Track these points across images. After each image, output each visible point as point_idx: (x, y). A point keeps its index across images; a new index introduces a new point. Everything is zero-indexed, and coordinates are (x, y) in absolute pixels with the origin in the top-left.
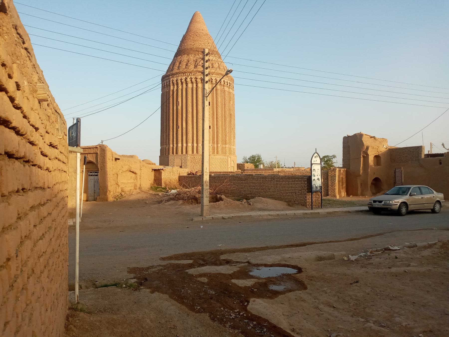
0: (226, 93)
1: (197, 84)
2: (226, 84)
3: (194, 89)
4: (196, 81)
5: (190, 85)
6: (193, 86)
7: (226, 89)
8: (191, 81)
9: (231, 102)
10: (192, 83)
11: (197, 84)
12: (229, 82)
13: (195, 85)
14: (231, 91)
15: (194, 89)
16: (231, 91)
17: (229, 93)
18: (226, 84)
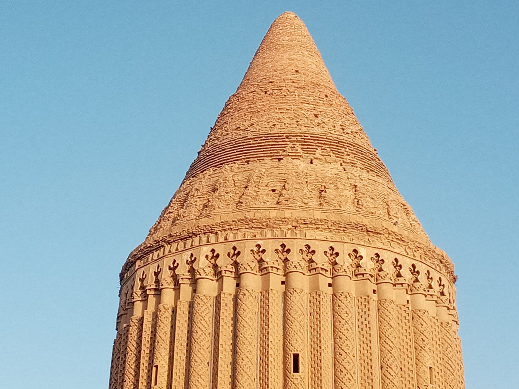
0: (393, 314)
1: (238, 276)
2: (389, 269)
3: (227, 301)
4: (236, 264)
5: (208, 287)
6: (221, 288)
7: (390, 293)
8: (215, 266)
9: (428, 360)
10: (218, 275)
11: (238, 276)
12: (406, 263)
13: (229, 284)
14: (422, 303)
15: (227, 301)
16: (422, 303)
17: (415, 315)
18: (389, 269)
